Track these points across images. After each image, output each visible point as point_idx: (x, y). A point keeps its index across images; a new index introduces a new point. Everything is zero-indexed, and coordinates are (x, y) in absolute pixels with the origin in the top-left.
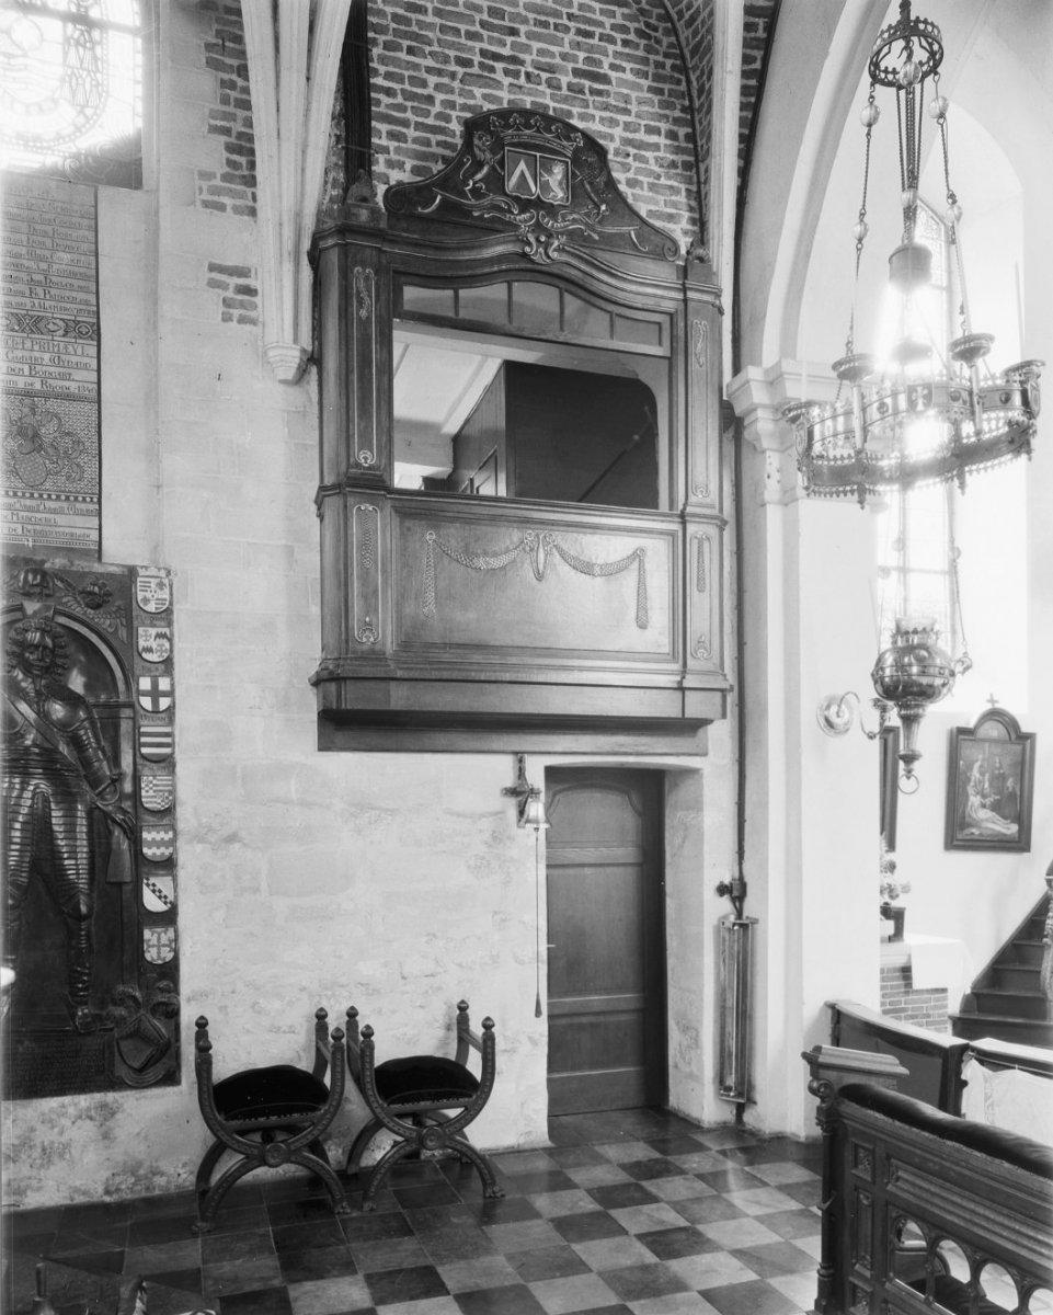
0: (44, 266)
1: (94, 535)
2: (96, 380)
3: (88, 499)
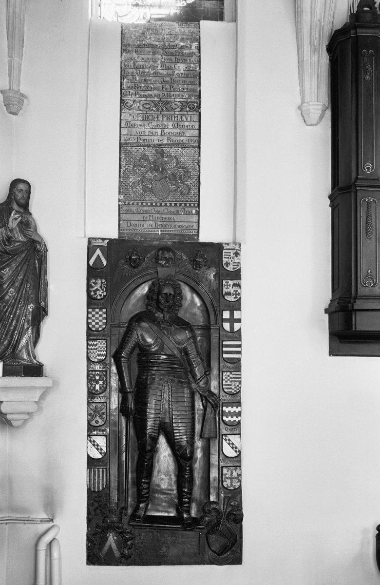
0: (170, 72)
1: (195, 226)
2: (198, 135)
3: (192, 205)
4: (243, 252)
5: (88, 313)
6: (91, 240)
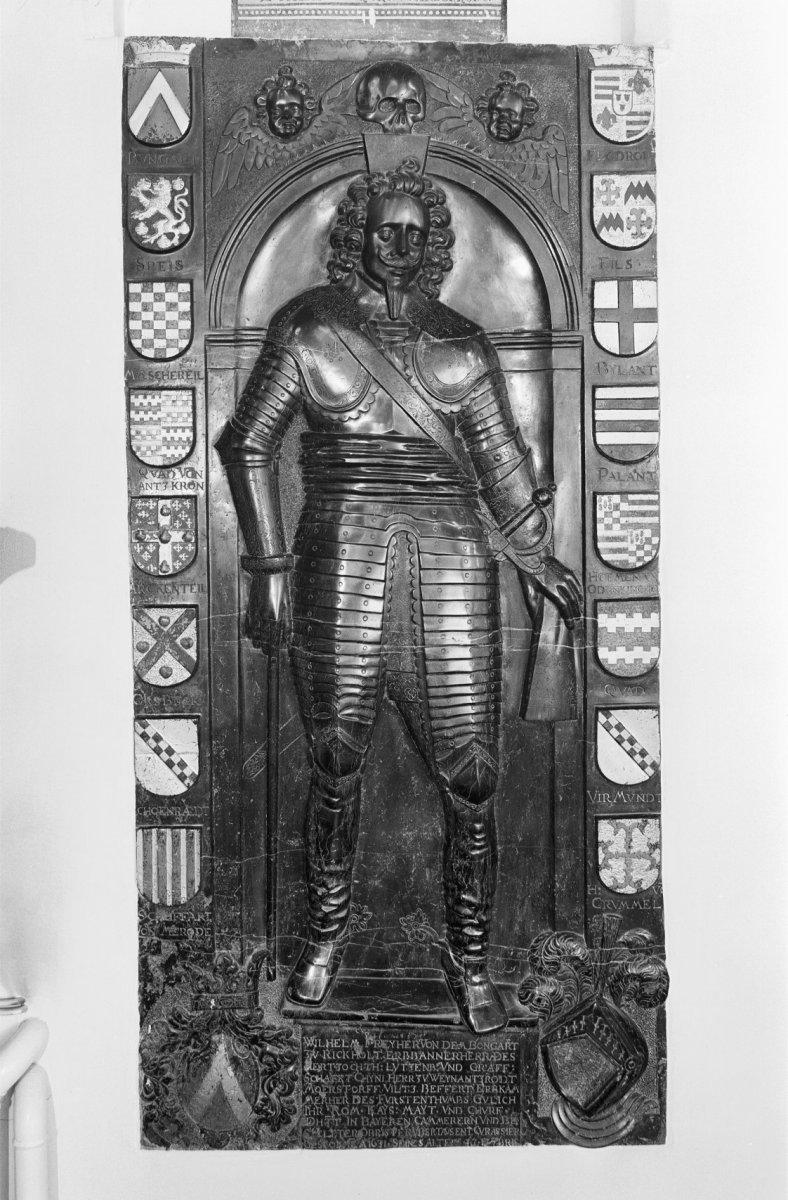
4: (660, 78)
5: (127, 298)
6: (134, 44)
